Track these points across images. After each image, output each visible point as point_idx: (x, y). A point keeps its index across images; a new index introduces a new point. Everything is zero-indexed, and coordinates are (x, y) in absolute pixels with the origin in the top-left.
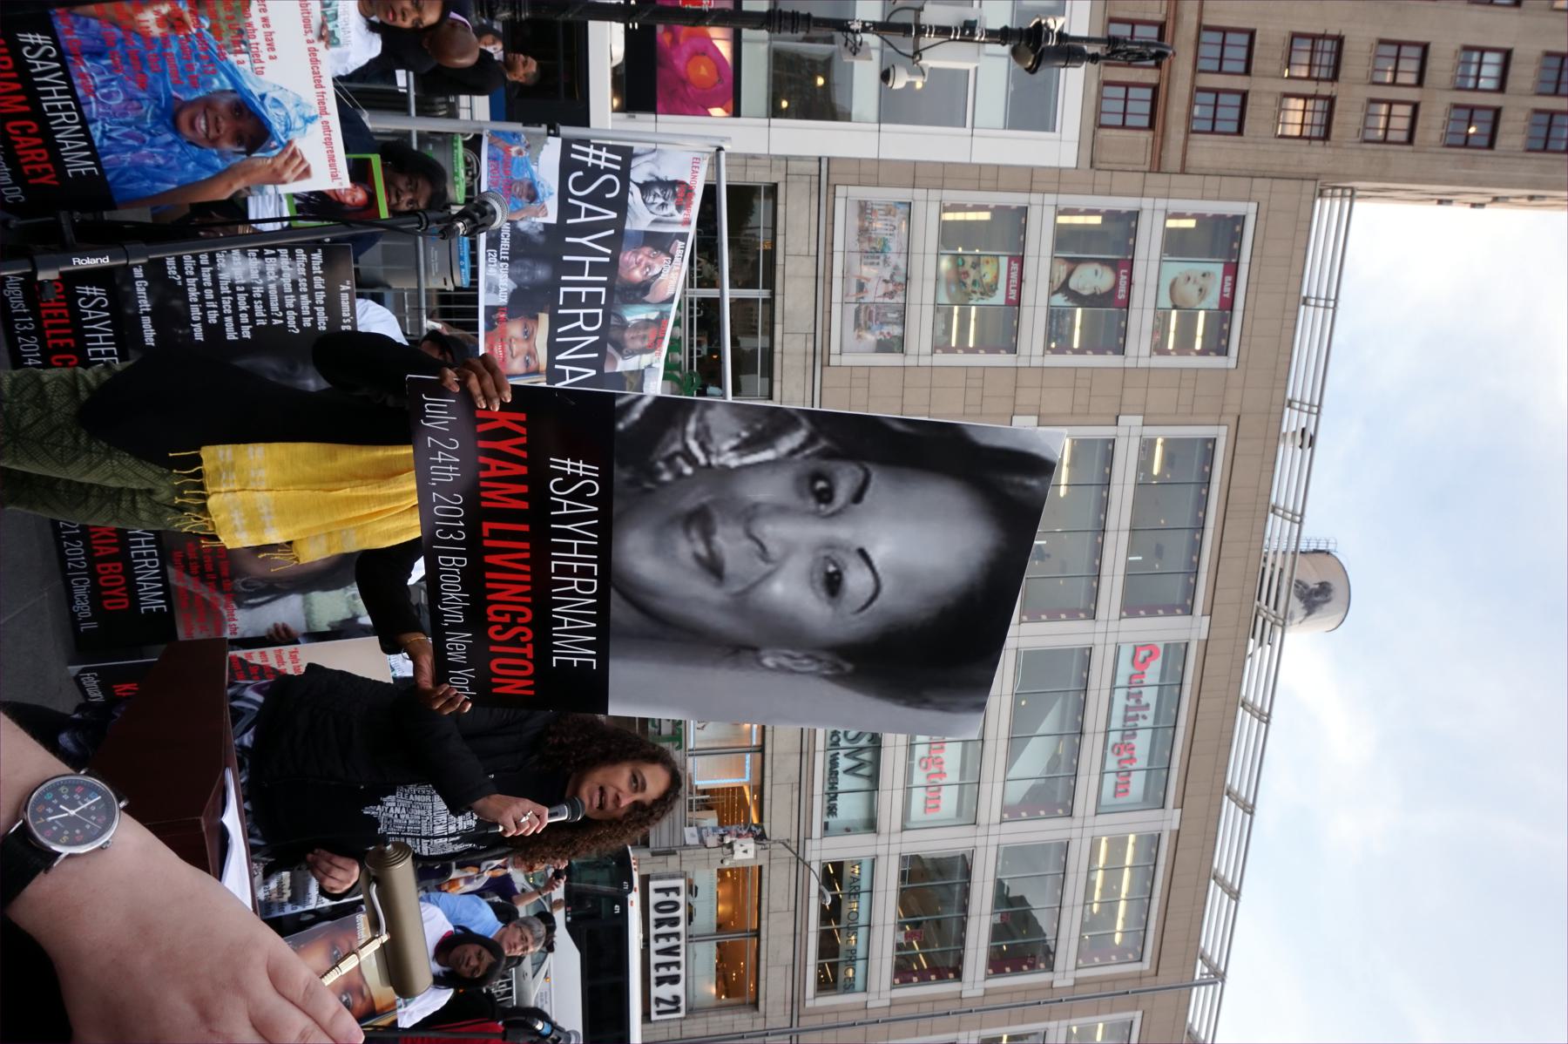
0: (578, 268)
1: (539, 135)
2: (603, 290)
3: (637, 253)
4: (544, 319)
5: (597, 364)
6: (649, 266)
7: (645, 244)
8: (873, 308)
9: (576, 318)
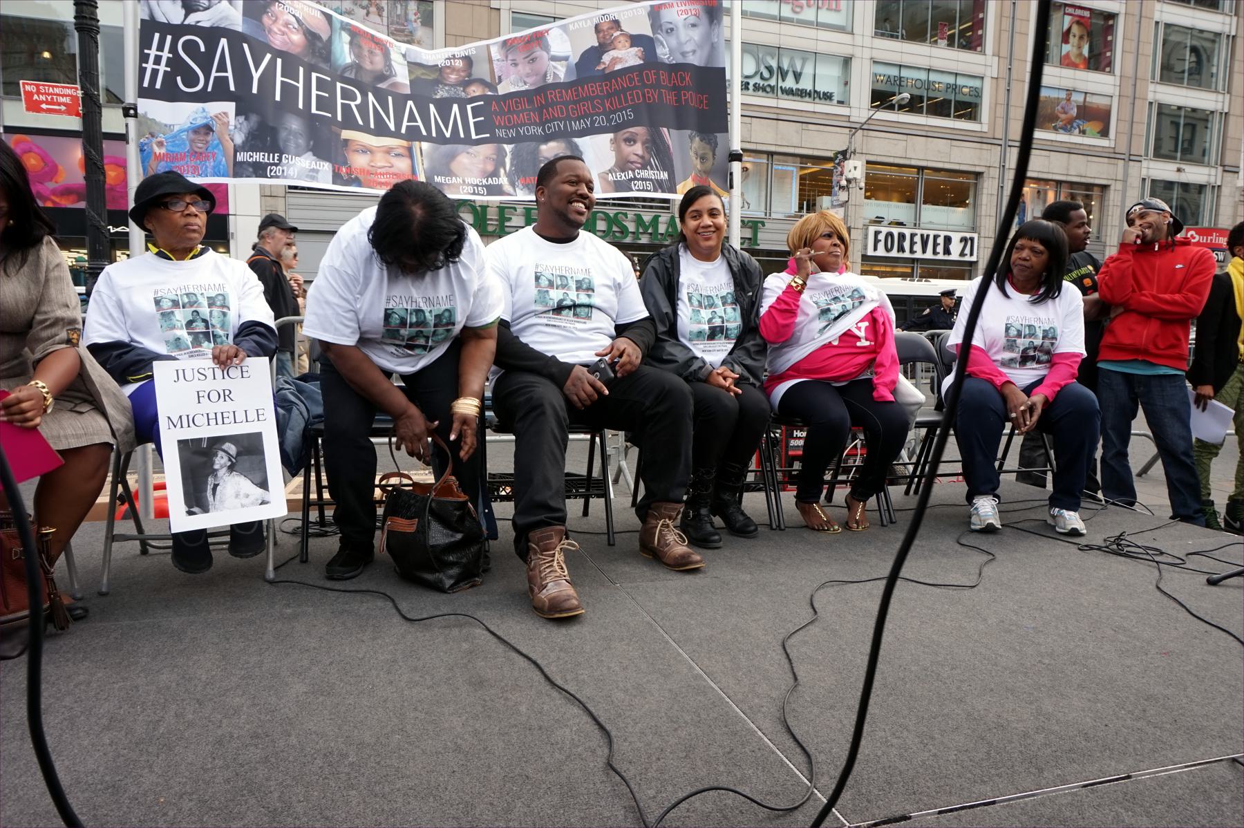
0: (289, 91)
1: (139, 125)
2: (314, 75)
3: (270, 31)
4: (346, 134)
5: (400, 101)
6: (287, 24)
7: (260, 20)
8: (393, 27)
9: (346, 108)
